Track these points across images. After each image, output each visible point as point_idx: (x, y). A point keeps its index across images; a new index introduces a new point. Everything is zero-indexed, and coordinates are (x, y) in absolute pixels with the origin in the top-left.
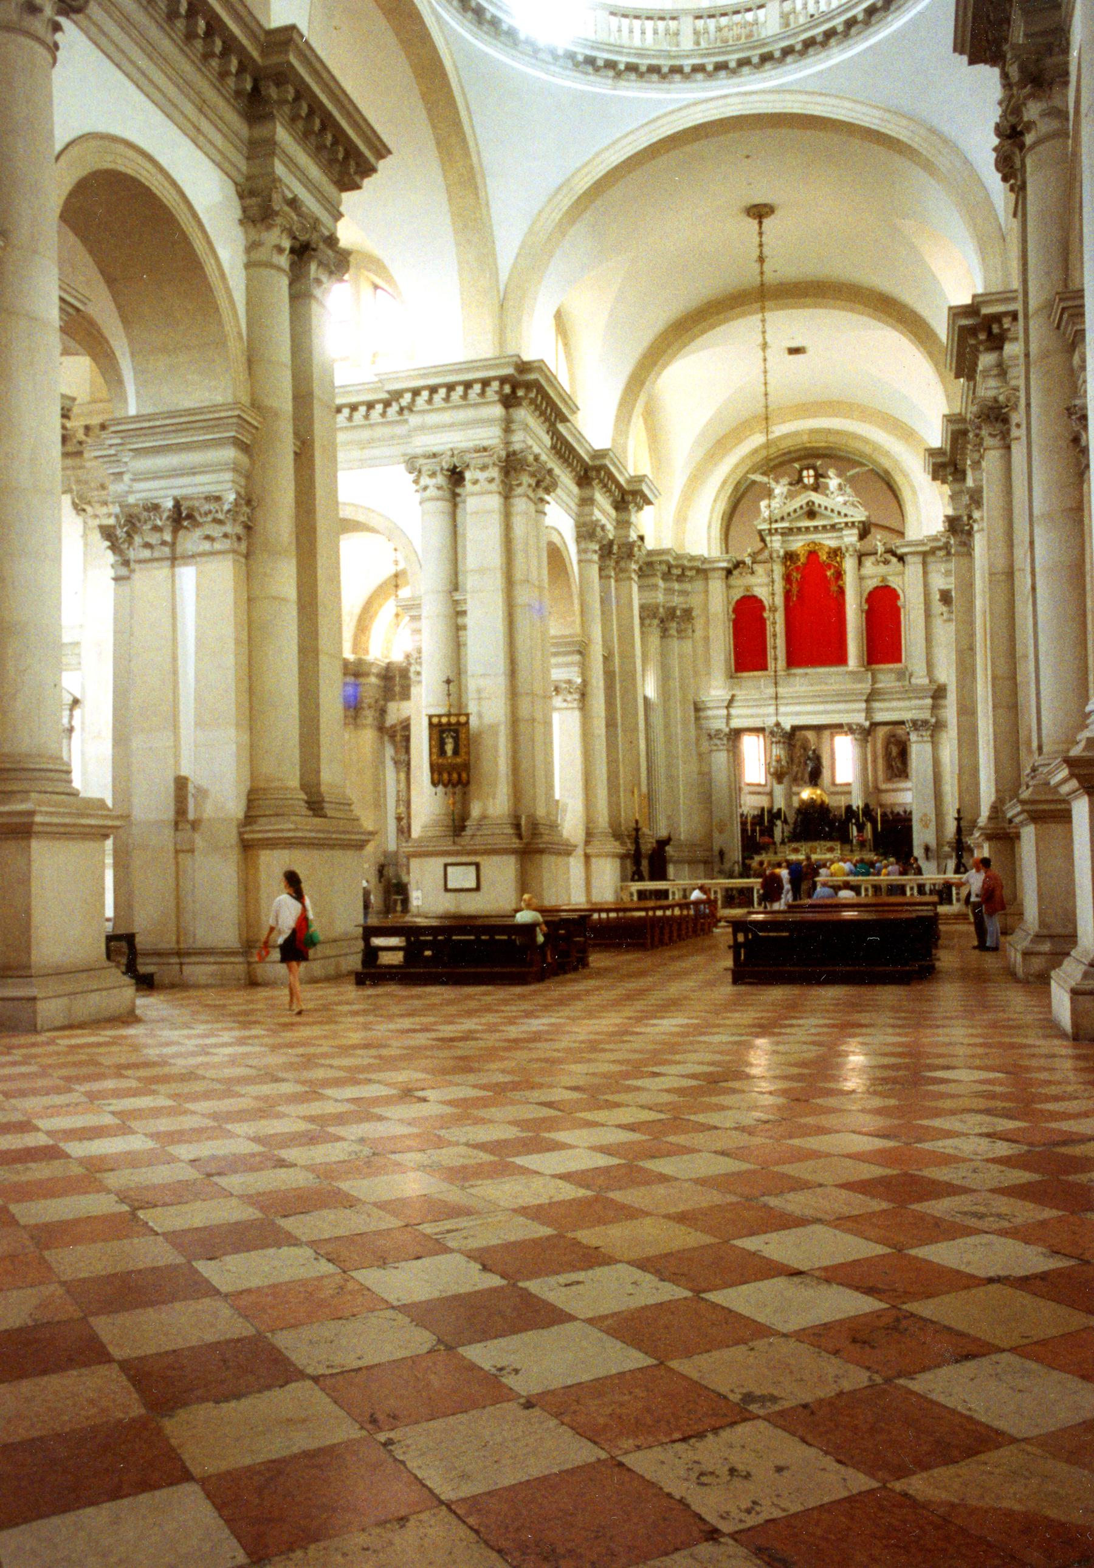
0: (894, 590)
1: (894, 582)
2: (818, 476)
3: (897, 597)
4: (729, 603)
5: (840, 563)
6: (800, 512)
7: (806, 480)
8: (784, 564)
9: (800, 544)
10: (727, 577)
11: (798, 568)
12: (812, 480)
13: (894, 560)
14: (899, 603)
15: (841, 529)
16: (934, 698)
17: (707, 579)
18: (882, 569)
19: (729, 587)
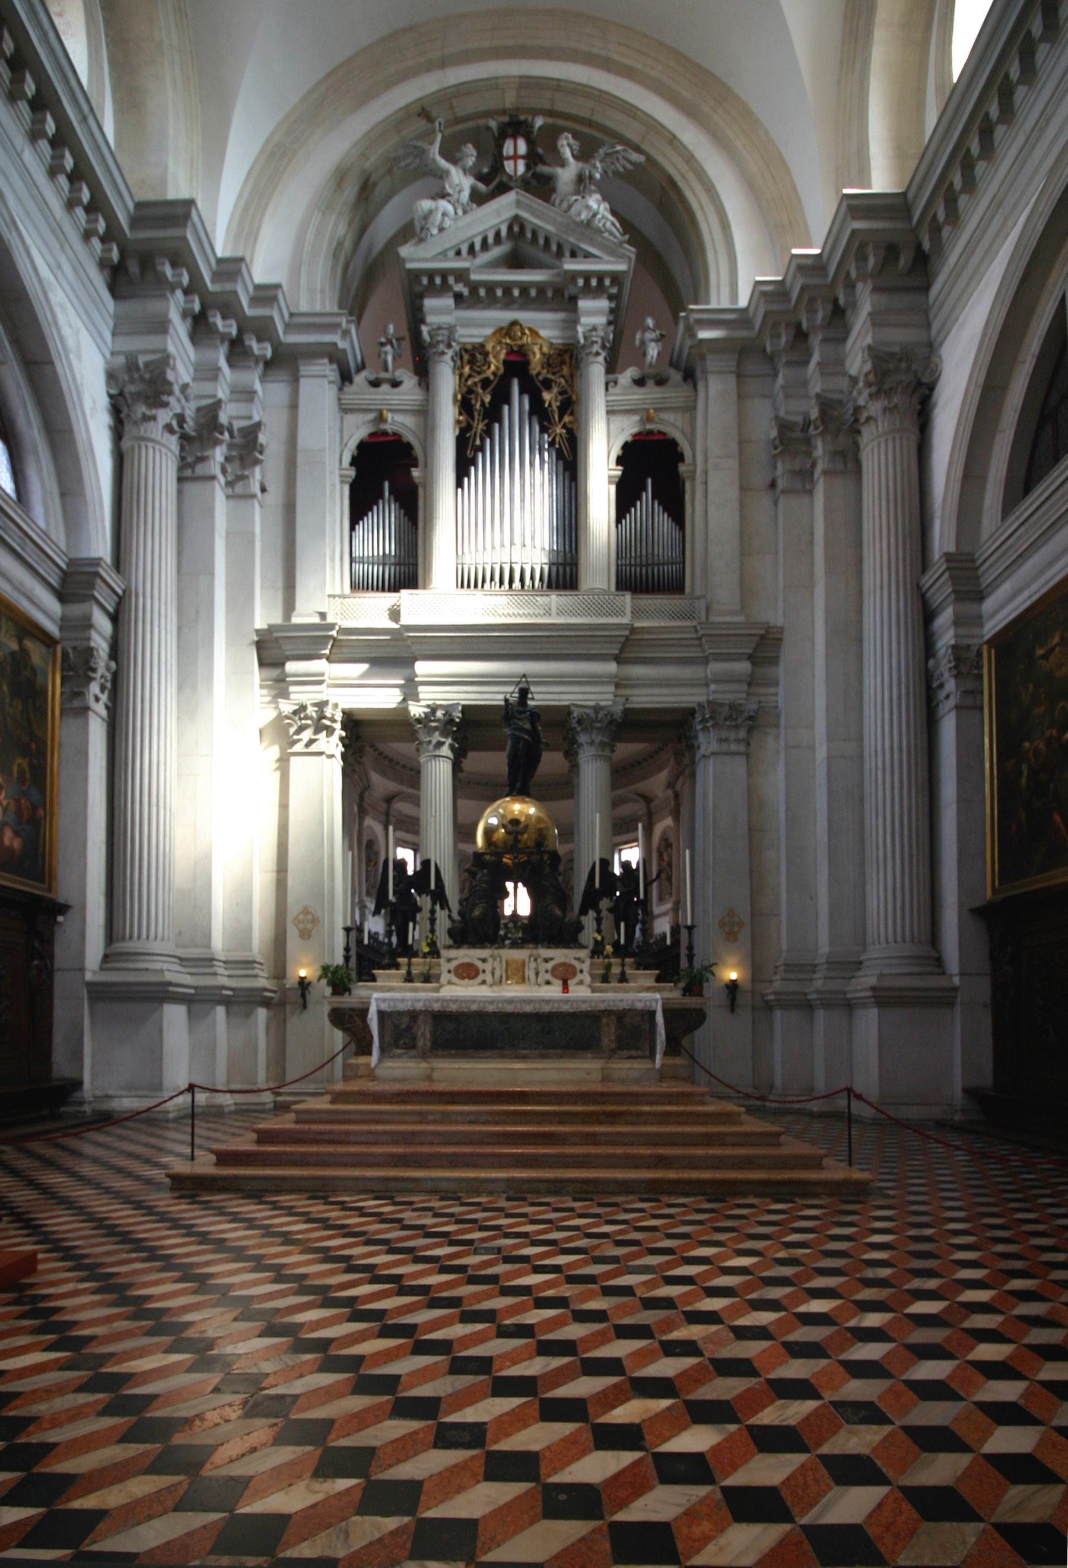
0: (673, 444)
1: (672, 425)
2: (532, 158)
3: (681, 458)
4: (343, 445)
5: (571, 379)
6: (496, 252)
7: (509, 166)
8: (458, 369)
9: (489, 331)
10: (341, 389)
11: (485, 383)
12: (521, 168)
13: (676, 376)
14: (682, 468)
15: (573, 299)
16: (750, 657)
17: (295, 380)
18: (650, 394)
19: (345, 409)
